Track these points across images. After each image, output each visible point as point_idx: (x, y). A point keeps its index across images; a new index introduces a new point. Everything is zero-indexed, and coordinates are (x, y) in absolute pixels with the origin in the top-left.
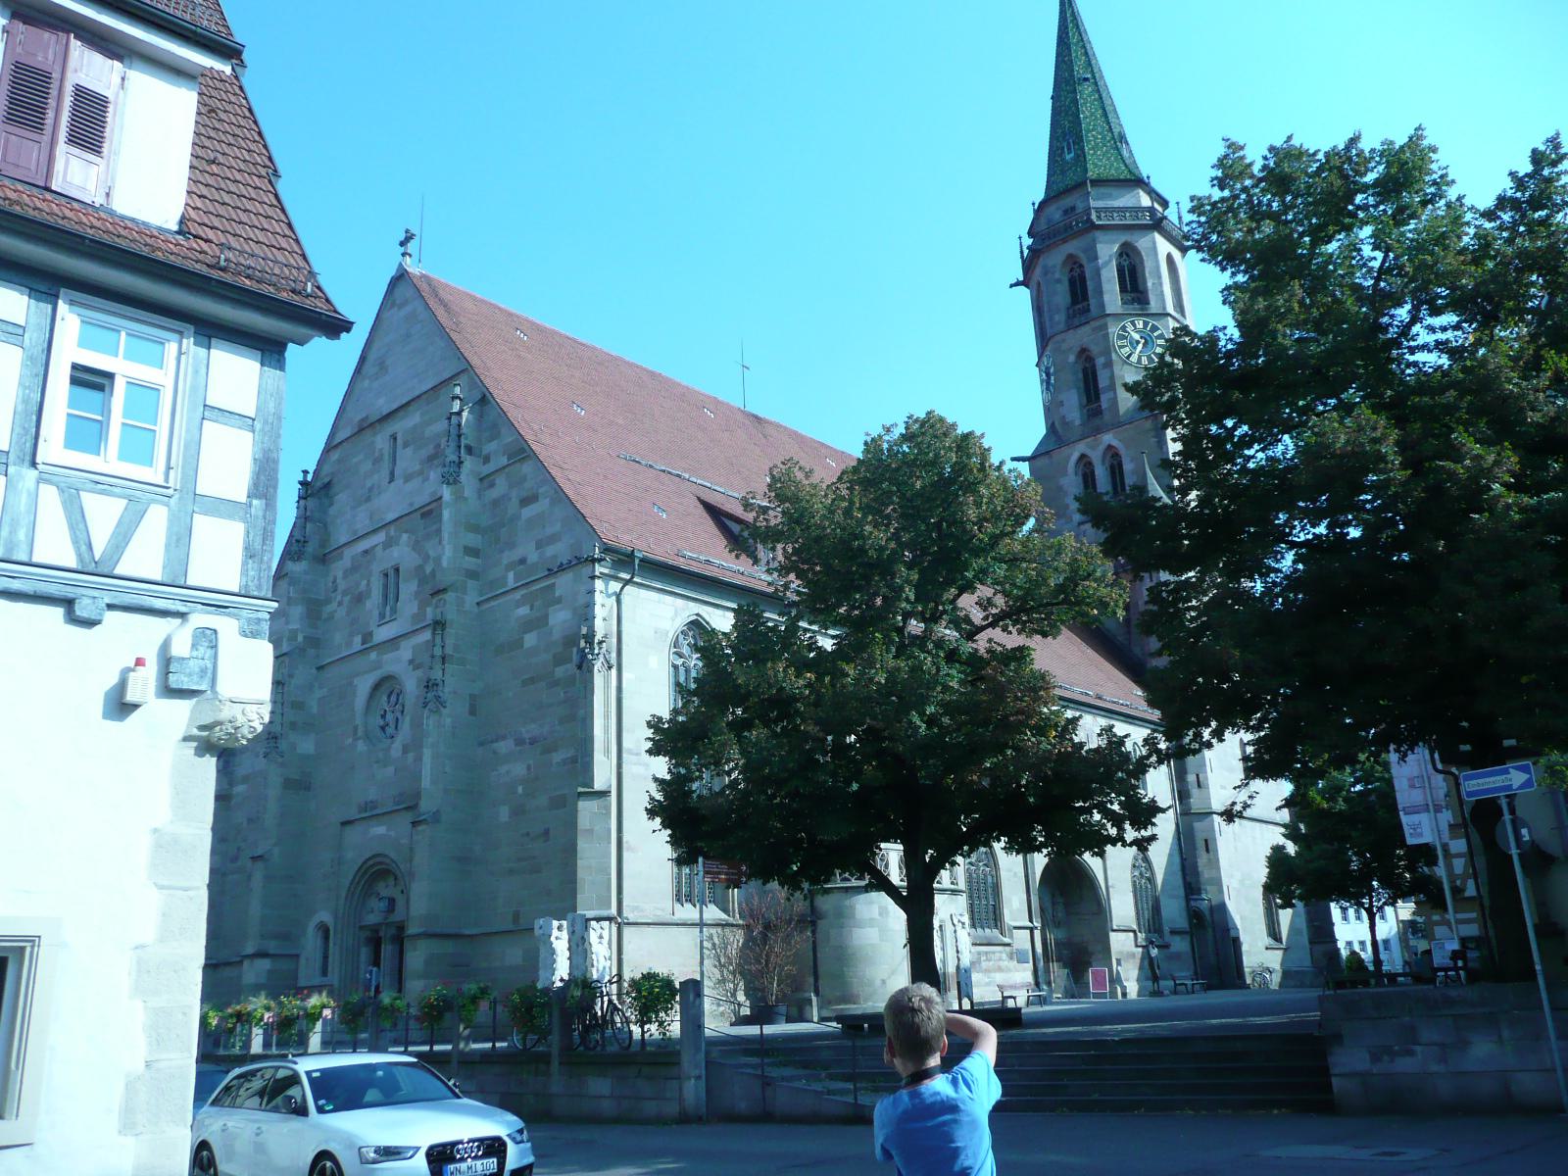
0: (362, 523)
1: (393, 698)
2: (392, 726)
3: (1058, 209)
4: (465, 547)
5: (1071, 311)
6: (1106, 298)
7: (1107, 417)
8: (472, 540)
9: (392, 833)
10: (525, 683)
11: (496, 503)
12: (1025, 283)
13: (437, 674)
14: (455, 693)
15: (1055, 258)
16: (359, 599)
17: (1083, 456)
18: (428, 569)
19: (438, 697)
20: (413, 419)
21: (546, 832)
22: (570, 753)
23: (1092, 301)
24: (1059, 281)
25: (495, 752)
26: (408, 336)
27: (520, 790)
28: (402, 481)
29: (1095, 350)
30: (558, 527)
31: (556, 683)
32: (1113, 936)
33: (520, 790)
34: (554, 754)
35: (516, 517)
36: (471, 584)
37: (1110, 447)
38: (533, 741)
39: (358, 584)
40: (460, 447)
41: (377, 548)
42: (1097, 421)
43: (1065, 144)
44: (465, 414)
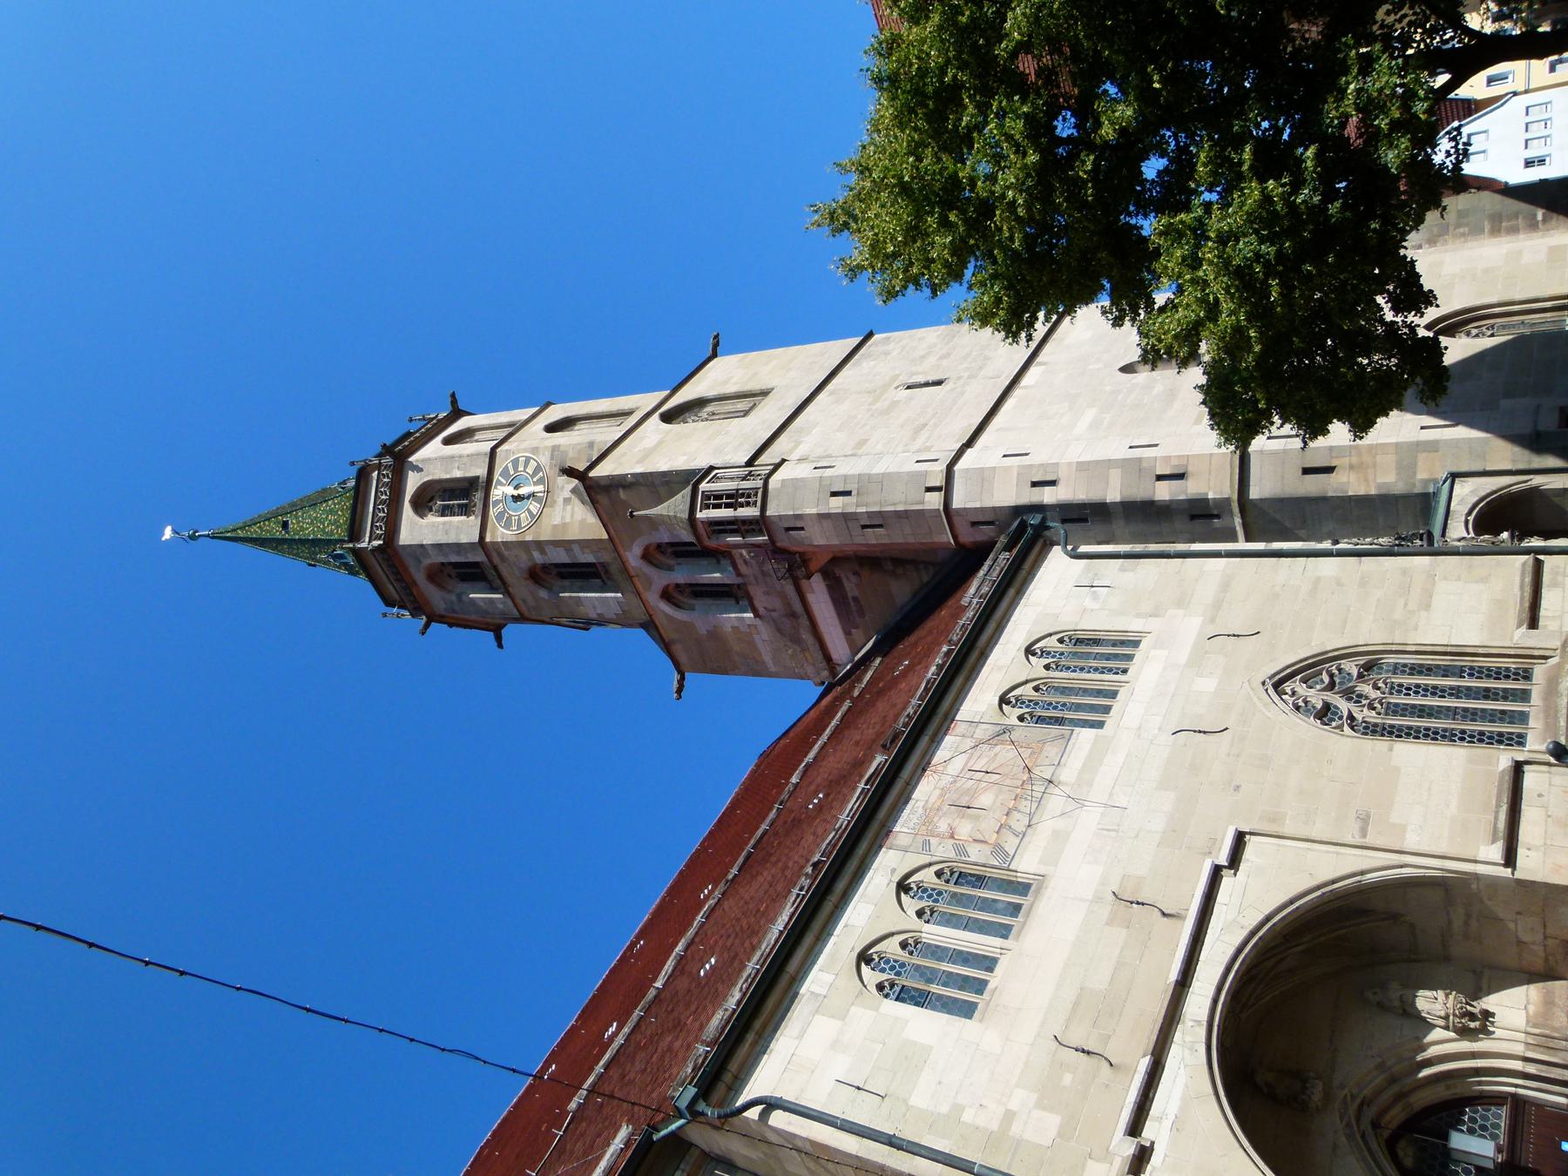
7: (606, 557)
12: (497, 631)
15: (436, 597)
32: (1533, 865)
37: (646, 556)
42: (614, 569)
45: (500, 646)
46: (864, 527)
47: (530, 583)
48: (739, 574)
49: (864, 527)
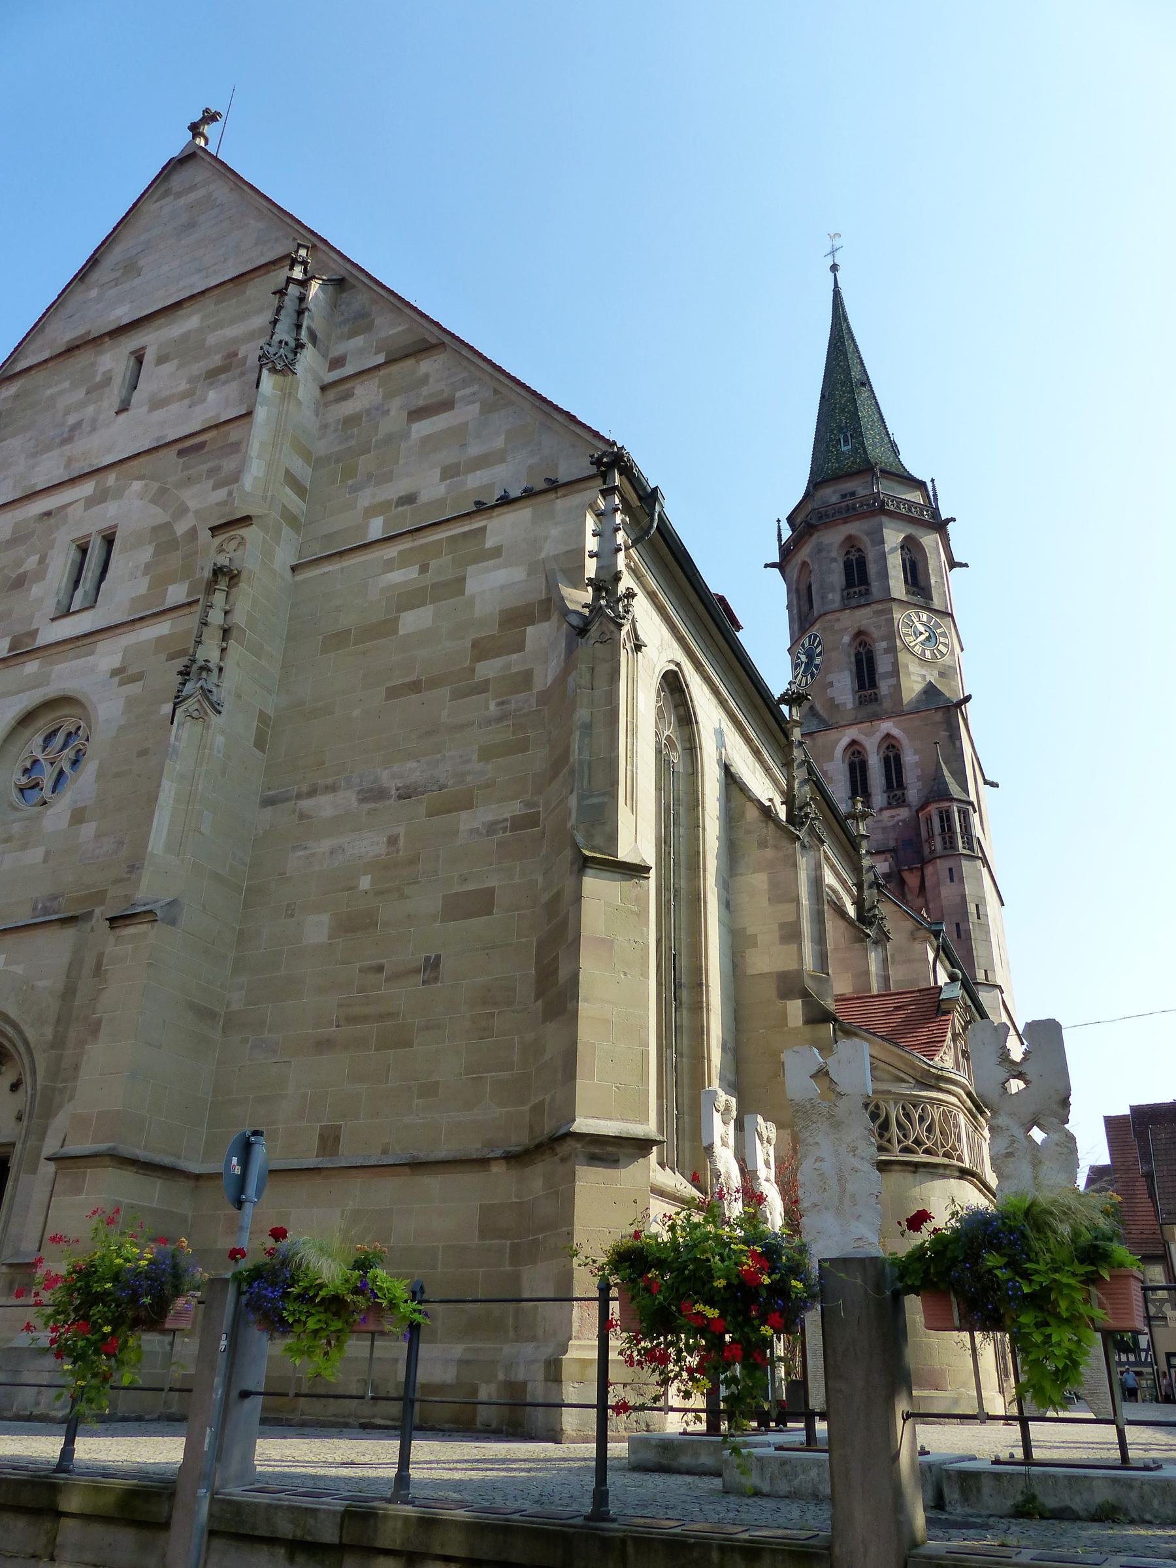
0: (50, 469)
1: (60, 739)
2: (47, 782)
3: (834, 492)
4: (287, 472)
5: (845, 593)
6: (892, 583)
8: (299, 467)
9: (19, 969)
10: (393, 693)
11: (350, 421)
13: (209, 652)
14: (239, 697)
15: (833, 538)
16: (20, 583)
17: (853, 743)
18: (181, 528)
19: (206, 693)
20: (189, 322)
21: (433, 965)
22: (515, 808)
23: (875, 586)
24: (834, 560)
25: (302, 816)
26: (192, 225)
27: (365, 883)
28: (145, 408)
29: (876, 633)
30: (499, 442)
31: (483, 687)
33: (365, 883)
34: (464, 815)
35: (406, 435)
36: (286, 531)
37: (888, 736)
38: (406, 794)
39: (19, 563)
40: (298, 327)
41: (70, 510)
42: (874, 707)
43: (841, 437)
44: (315, 287)
45: (766, 566)
46: (958, 925)
47: (856, 630)
48: (881, 810)
49: (958, 925)
